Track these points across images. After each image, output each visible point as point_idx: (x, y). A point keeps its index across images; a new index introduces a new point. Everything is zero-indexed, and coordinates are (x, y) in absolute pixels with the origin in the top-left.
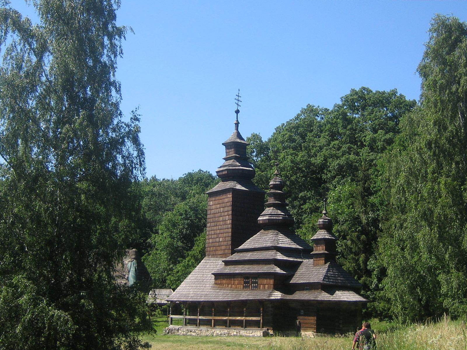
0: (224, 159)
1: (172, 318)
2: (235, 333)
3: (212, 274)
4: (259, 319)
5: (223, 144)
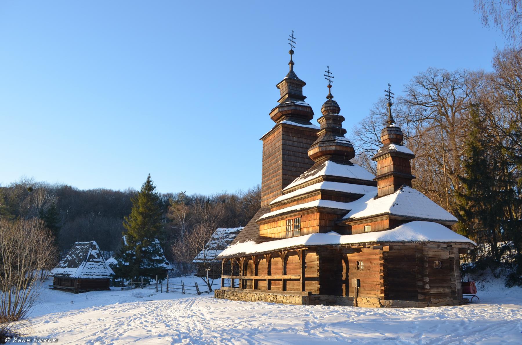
0: (278, 101)
4: (299, 278)
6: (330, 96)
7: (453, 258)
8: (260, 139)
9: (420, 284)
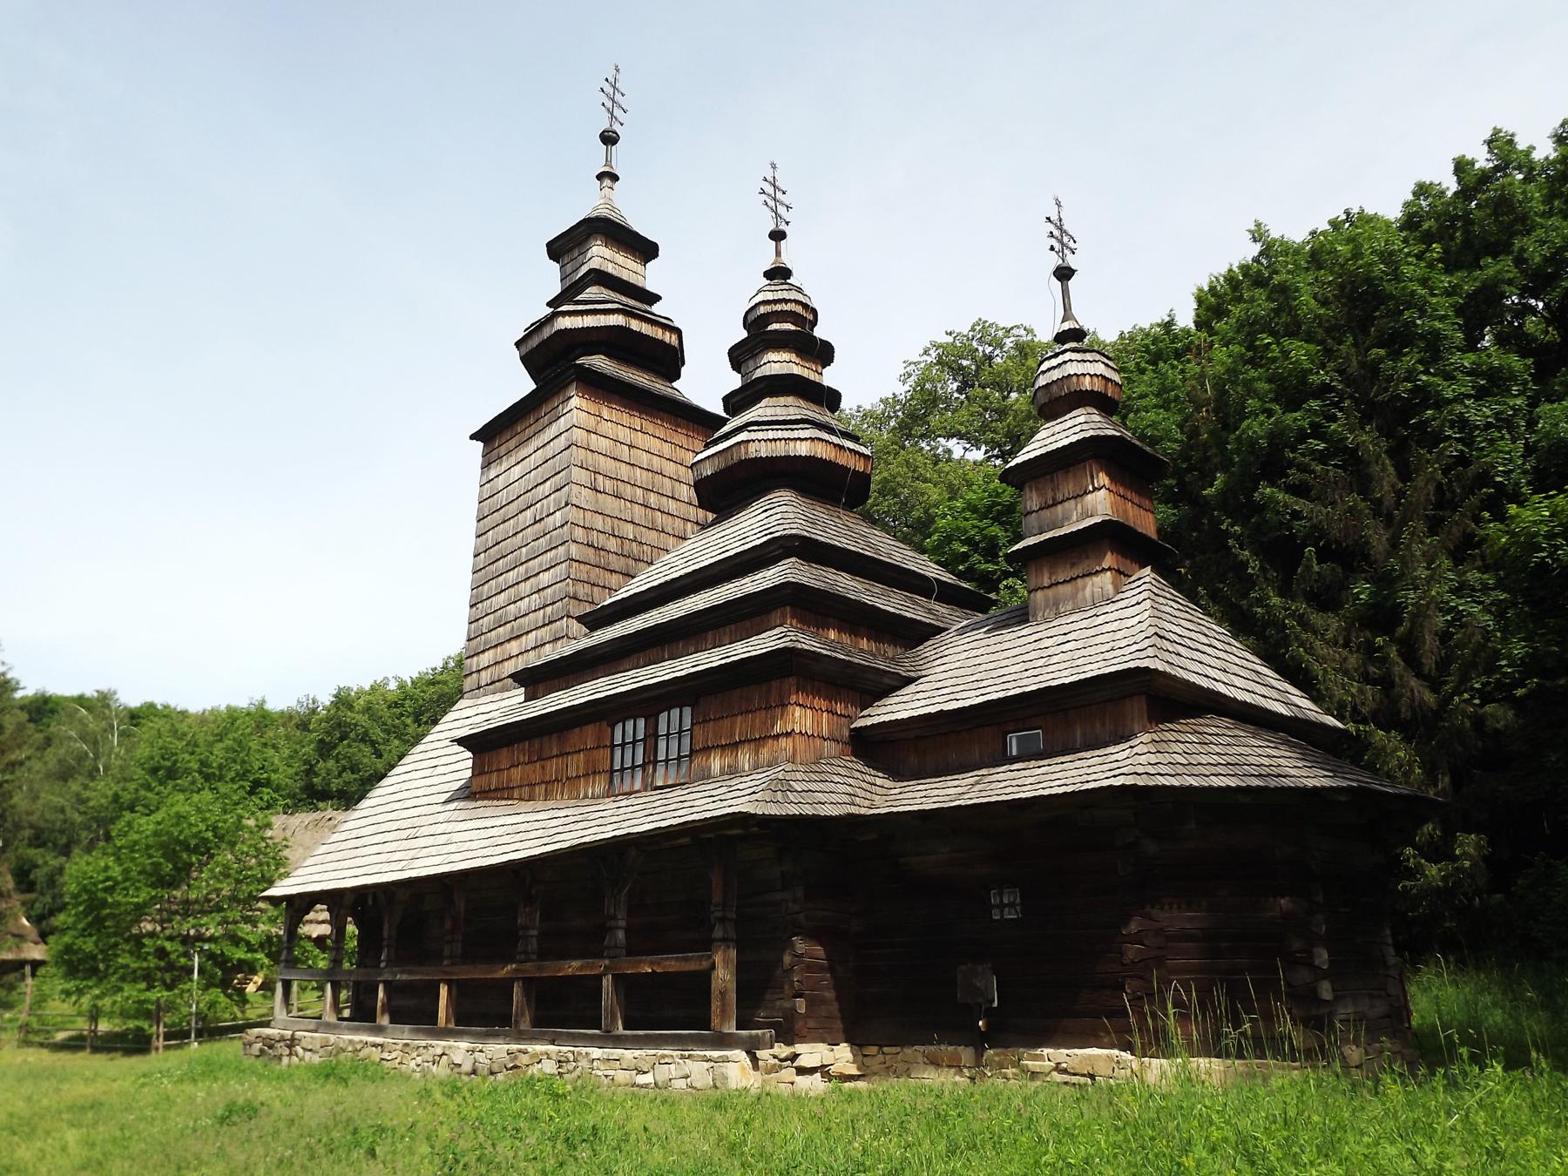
2: (549, 1067)
3: (461, 741)
4: (705, 964)
6: (779, 274)
8: (473, 437)
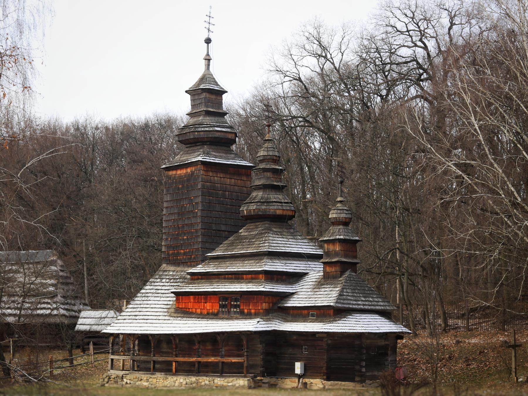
1: (112, 360)
2: (207, 382)
3: (172, 292)
4: (243, 361)
5: (186, 92)
7: (388, 345)
9: (357, 367)
